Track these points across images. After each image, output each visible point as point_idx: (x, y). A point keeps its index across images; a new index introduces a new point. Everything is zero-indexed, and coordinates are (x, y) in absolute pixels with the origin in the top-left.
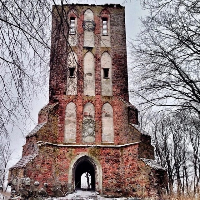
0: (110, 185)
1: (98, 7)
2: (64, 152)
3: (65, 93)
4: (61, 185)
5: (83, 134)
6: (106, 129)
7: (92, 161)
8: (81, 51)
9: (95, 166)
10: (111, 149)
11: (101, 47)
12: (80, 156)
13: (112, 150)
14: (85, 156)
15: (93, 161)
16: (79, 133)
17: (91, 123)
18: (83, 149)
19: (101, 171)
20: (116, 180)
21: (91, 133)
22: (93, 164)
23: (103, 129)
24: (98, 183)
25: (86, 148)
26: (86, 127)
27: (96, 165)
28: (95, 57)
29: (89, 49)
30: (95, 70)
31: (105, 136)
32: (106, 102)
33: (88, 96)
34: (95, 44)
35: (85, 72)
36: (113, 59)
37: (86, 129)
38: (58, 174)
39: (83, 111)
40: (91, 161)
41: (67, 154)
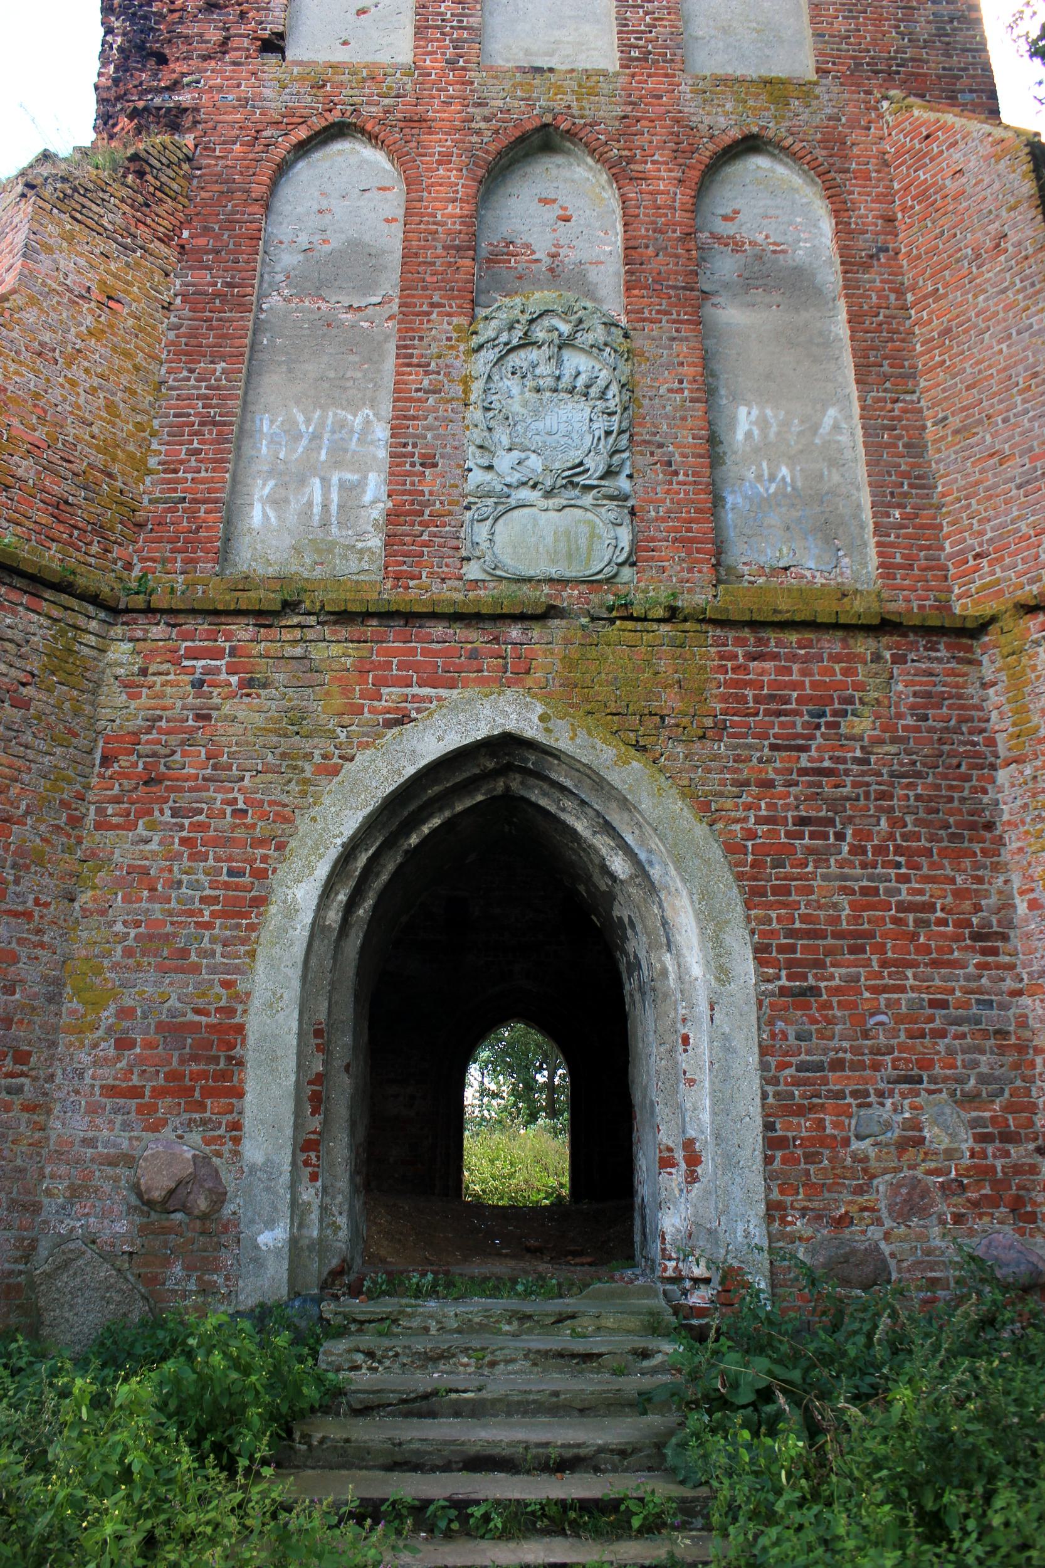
0: (881, 1184)
2: (198, 684)
3: (274, 45)
4: (136, 1188)
5: (477, 477)
7: (608, 828)
9: (652, 888)
10: (864, 646)
12: (431, 741)
13: (877, 658)
14: (505, 748)
15: (616, 818)
17: (566, 343)
18: (475, 637)
19: (745, 966)
20: (970, 1100)
21: (575, 456)
22: (619, 865)
24: (693, 1160)
25: (515, 632)
26: (512, 385)
27: (655, 872)
31: (764, 504)
33: (539, 70)
37: (516, 407)
38: (96, 1005)
40: (580, 827)
41: (243, 717)
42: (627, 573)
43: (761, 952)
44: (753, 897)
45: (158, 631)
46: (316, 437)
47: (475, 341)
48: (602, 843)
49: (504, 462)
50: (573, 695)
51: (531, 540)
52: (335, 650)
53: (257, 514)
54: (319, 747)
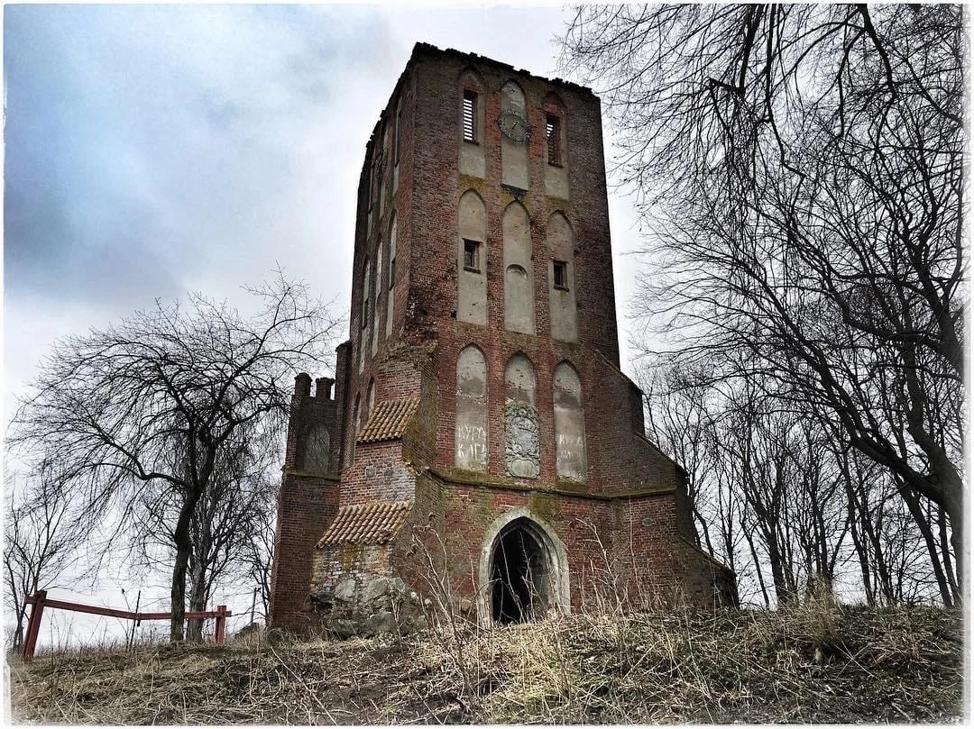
1: (537, 81)
3: (454, 315)
5: (508, 451)
6: (565, 439)
8: (495, 197)
10: (589, 502)
11: (547, 196)
12: (510, 518)
16: (497, 445)
18: (517, 495)
22: (541, 545)
23: (559, 439)
28: (532, 223)
29: (518, 194)
30: (533, 259)
31: (564, 461)
32: (565, 361)
34: (531, 183)
35: (507, 264)
36: (576, 238)
39: (504, 377)
41: (473, 508)
42: (539, 477)
43: (570, 565)
44: (569, 555)
45: (453, 487)
46: (471, 434)
47: (507, 413)
48: (537, 540)
49: (514, 447)
50: (536, 509)
51: (521, 467)
52: (491, 495)
53: (460, 454)
54: (488, 517)
